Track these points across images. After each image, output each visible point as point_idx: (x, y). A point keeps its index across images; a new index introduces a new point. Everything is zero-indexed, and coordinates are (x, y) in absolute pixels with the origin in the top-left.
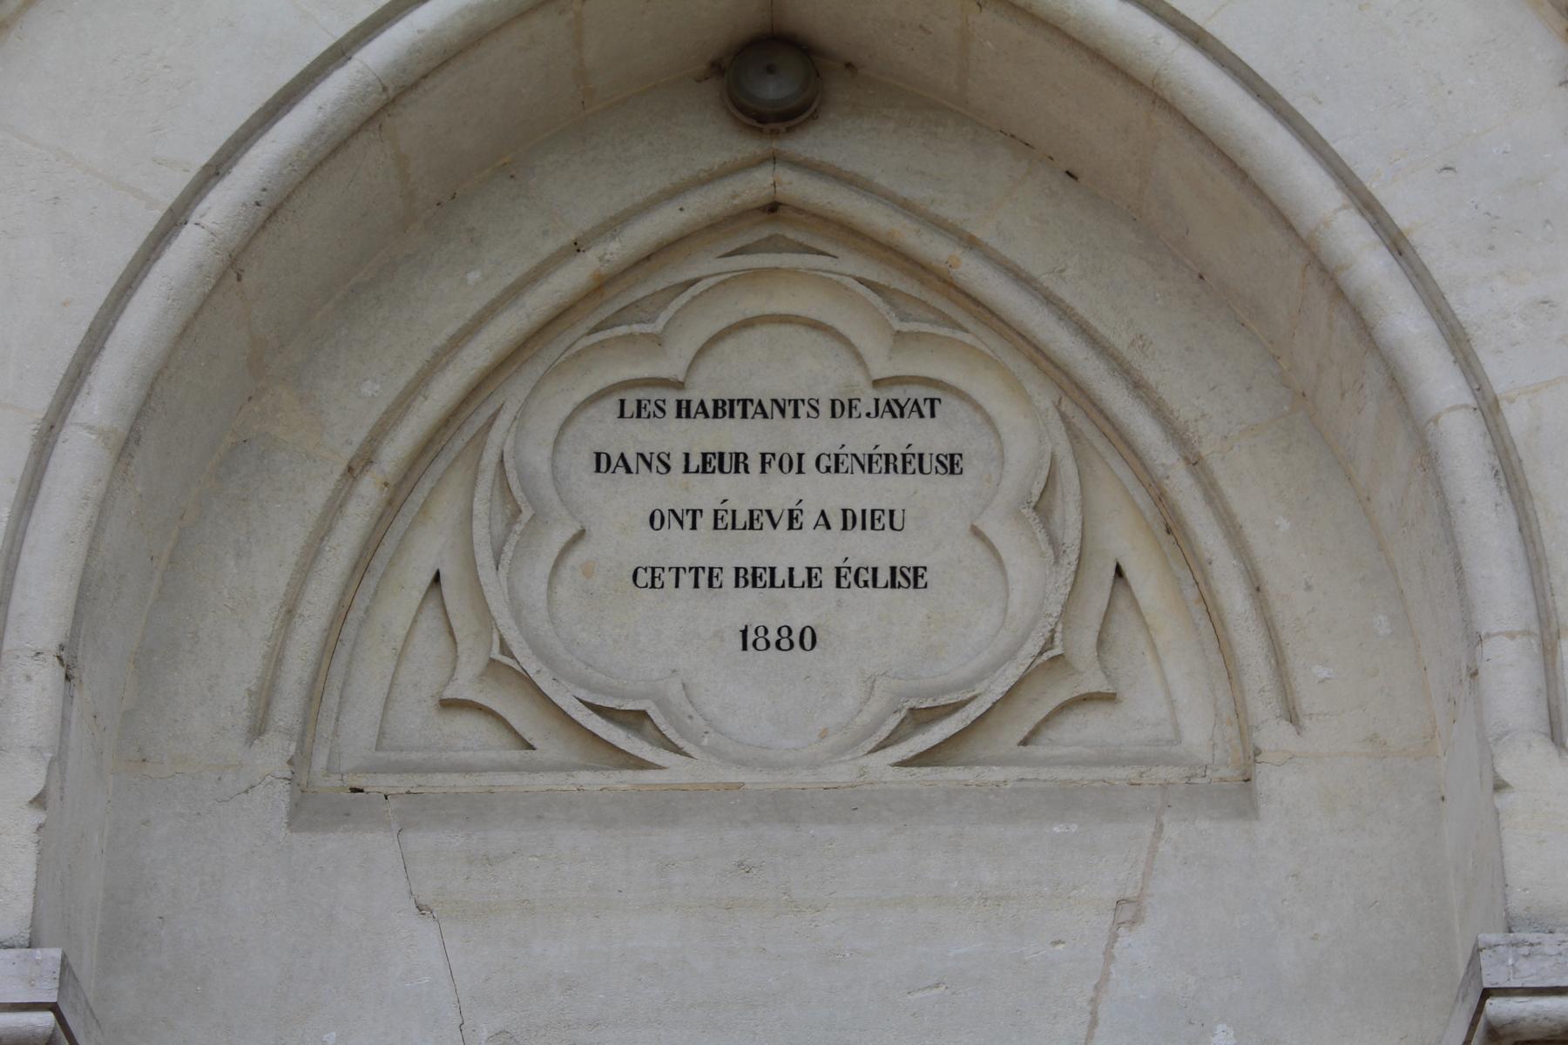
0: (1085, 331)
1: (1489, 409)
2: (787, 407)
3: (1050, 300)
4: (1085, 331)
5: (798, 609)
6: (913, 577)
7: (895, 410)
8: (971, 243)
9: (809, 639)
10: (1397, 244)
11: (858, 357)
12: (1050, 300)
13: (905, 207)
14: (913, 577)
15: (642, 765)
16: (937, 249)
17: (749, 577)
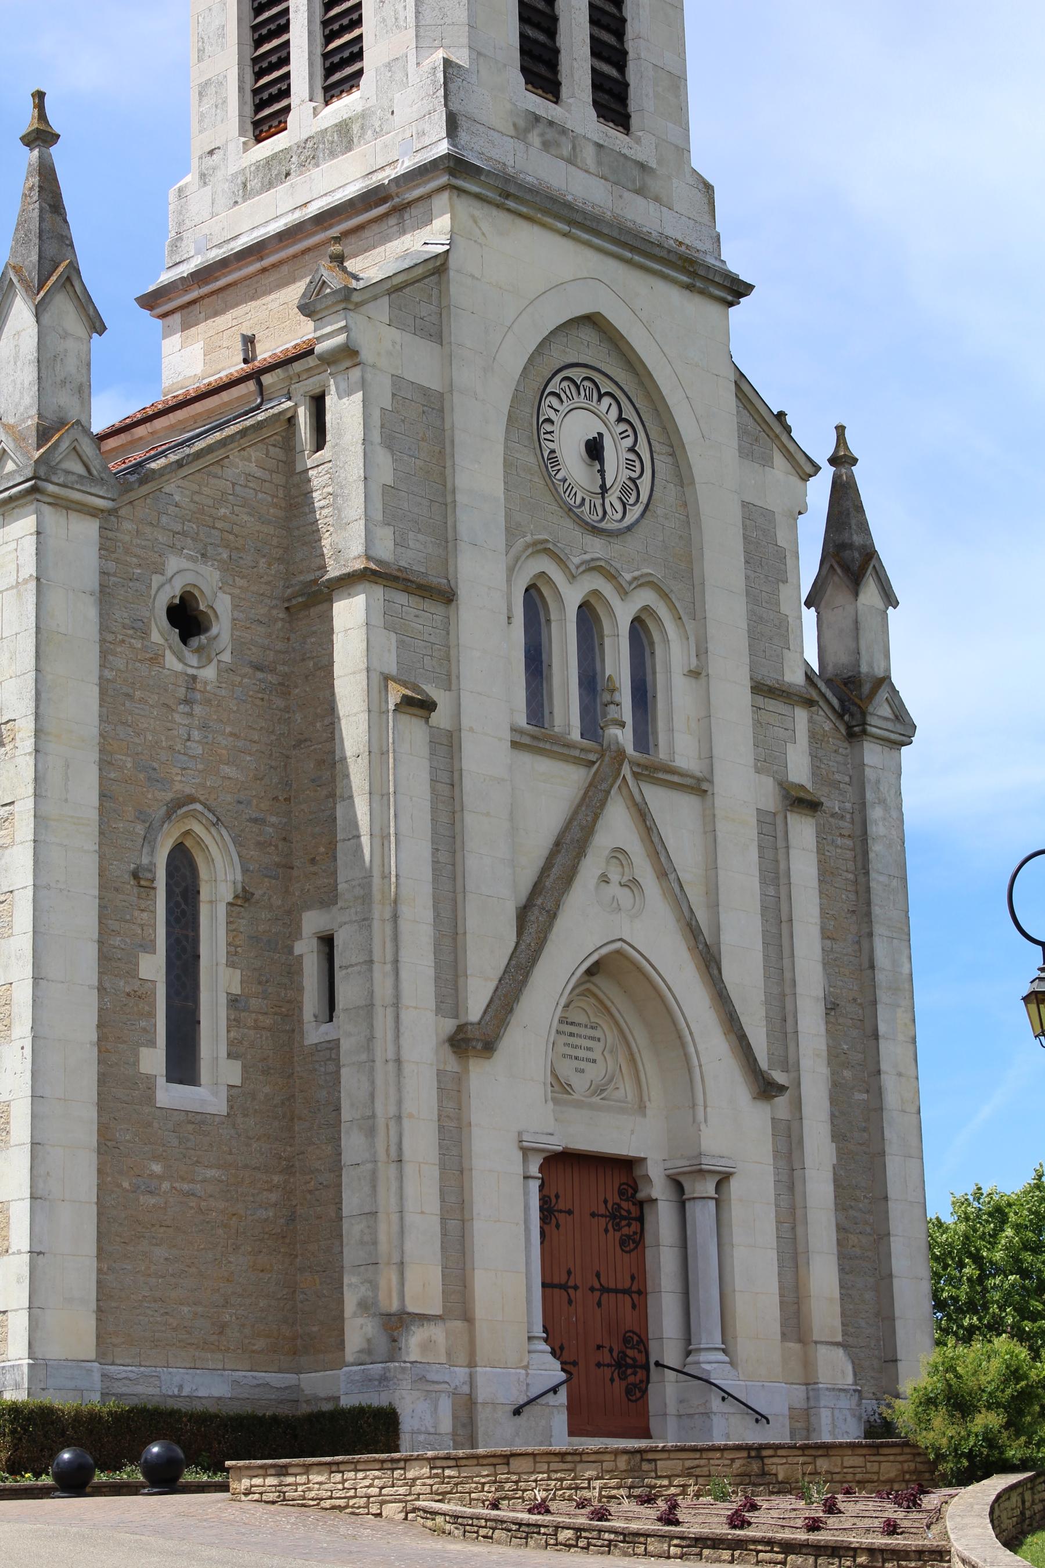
0: (626, 1022)
1: (700, 1066)
2: (579, 1025)
3: (623, 1017)
4: (626, 1022)
5: (582, 1065)
6: (594, 1061)
7: (592, 1028)
8: (613, 1003)
9: (582, 1071)
10: (691, 1033)
11: (589, 1017)
12: (623, 1017)
13: (604, 993)
14: (594, 1061)
15: (570, 1094)
16: (609, 1004)
17: (576, 1058)
